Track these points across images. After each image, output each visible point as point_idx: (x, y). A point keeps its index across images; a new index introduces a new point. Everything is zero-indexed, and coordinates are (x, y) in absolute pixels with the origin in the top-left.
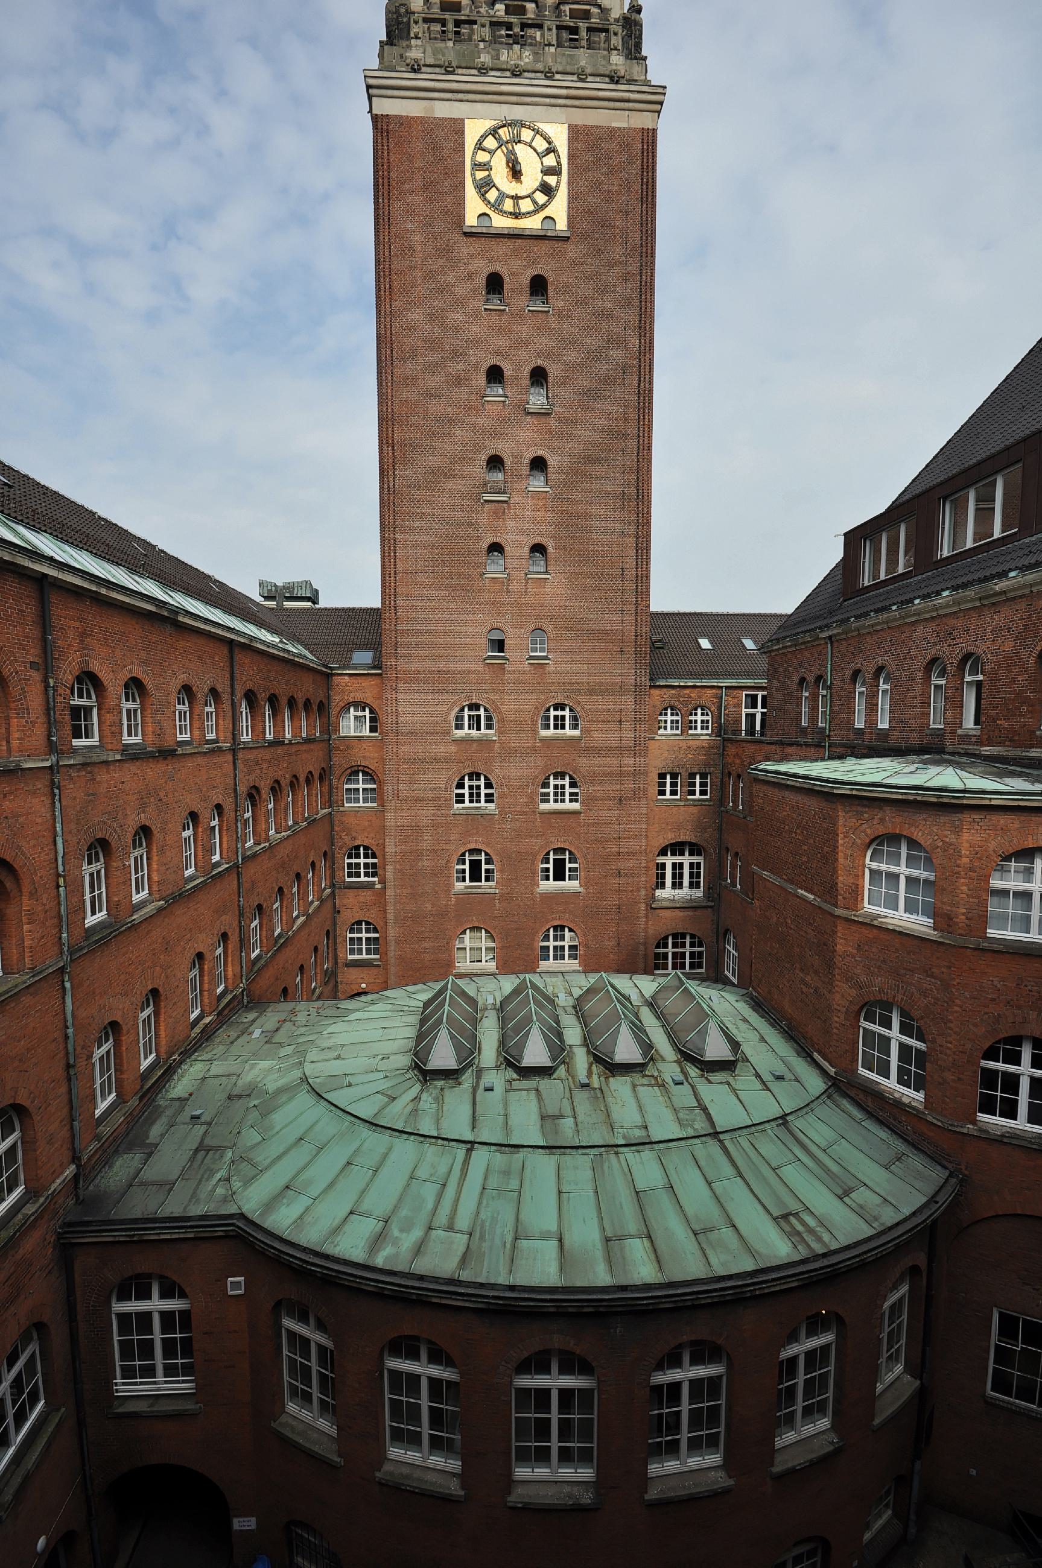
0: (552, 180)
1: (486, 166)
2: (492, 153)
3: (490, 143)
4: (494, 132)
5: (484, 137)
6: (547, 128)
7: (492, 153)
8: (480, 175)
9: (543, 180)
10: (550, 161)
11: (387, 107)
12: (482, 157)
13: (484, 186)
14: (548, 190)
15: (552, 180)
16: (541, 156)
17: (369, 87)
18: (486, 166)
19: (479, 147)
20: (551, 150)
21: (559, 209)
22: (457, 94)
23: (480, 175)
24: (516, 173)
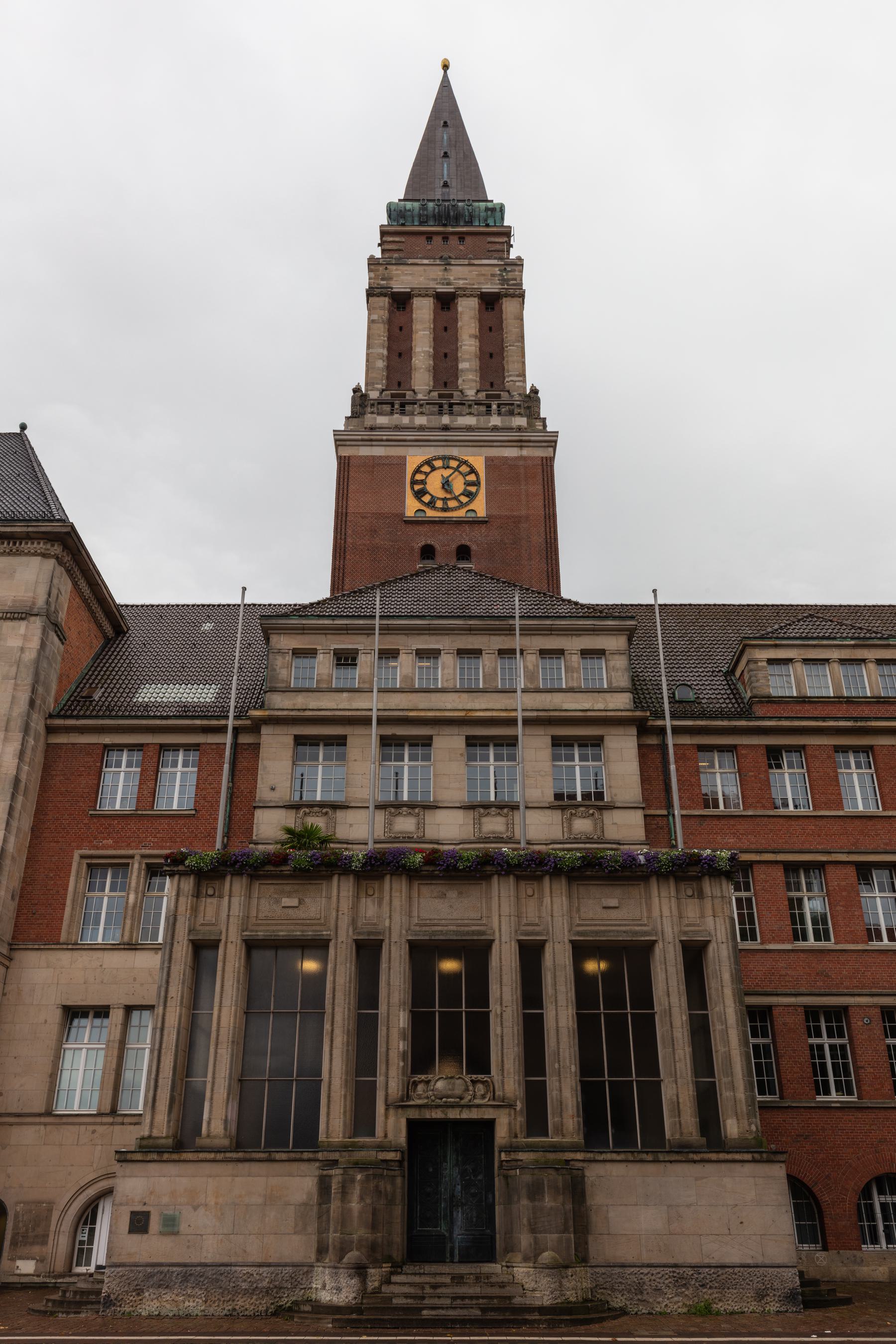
0: (473, 489)
1: (423, 482)
2: (427, 474)
3: (426, 469)
4: (428, 462)
5: (422, 466)
6: (471, 460)
7: (427, 474)
8: (417, 487)
9: (465, 490)
10: (472, 478)
11: (346, 452)
12: (419, 477)
13: (419, 495)
14: (471, 496)
15: (473, 489)
16: (464, 475)
17: (336, 440)
18: (423, 482)
19: (418, 471)
20: (473, 471)
21: (480, 507)
22: (402, 443)
23: (417, 487)
24: (446, 485)
